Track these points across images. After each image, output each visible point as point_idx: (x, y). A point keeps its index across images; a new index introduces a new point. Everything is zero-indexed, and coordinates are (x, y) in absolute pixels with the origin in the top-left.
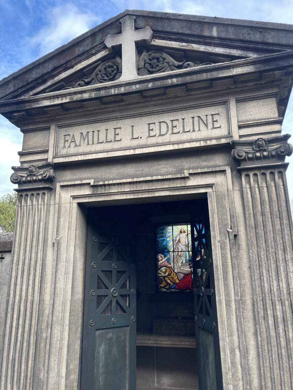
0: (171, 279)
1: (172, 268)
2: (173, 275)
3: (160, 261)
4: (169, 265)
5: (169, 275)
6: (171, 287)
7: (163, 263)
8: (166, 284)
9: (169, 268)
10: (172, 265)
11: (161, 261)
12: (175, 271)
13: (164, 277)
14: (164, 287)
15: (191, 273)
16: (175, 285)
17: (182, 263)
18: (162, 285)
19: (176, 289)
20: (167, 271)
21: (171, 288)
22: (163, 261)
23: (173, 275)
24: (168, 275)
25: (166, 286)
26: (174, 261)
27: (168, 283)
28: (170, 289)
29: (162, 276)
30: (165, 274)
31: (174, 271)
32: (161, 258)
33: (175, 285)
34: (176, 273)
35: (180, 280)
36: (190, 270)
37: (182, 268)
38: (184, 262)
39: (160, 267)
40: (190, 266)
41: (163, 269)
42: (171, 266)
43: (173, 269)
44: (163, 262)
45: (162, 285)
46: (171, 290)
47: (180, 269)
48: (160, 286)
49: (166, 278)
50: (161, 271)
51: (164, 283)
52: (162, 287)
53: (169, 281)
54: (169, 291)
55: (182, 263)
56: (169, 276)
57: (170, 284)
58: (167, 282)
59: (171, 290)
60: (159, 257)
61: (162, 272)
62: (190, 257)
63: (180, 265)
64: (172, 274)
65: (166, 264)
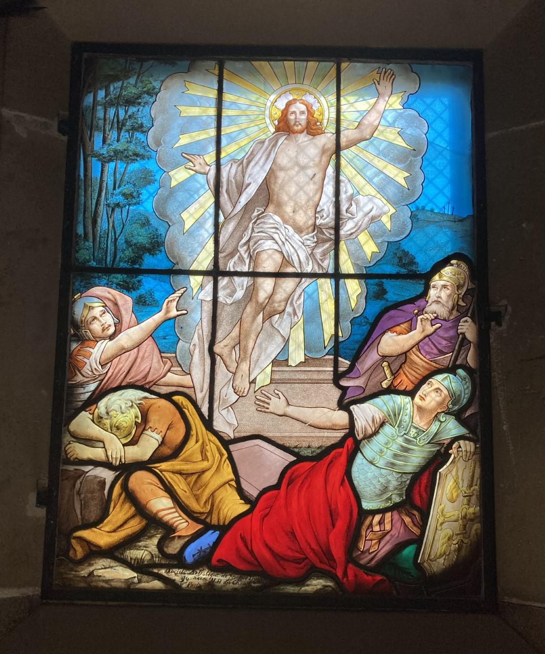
0: (180, 486)
1: (194, 403)
2: (203, 451)
3: (97, 339)
4: (171, 378)
5: (170, 452)
6: (173, 548)
7: (124, 363)
8: (135, 525)
9: (168, 397)
10: (199, 376)
11: (111, 337)
12: (218, 425)
13: (126, 469)
14: (114, 553)
15: (350, 441)
16: (210, 538)
17: (280, 362)
18: (101, 537)
19: (214, 569)
20: (153, 418)
21: (178, 561)
22: (130, 336)
23: (203, 451)
24: (157, 457)
25: (131, 541)
26: (217, 349)
27: (153, 523)
28: (169, 567)
29: (107, 465)
30: (134, 442)
31: (208, 423)
32: (108, 319)
33: (210, 538)
34: (227, 443)
35: (255, 493)
36: (341, 417)
37: (278, 405)
38: (297, 356)
39: (92, 387)
40: (344, 390)
41: (122, 406)
42: (186, 380)
43: (205, 410)
44: (124, 351)
45: (101, 537)
46: (176, 575)
47: (262, 407)
48: (81, 539)
49: (141, 482)
50: (98, 421)
51: (120, 512)
52: (95, 552)
53: (161, 504)
54: (157, 584)
55: (275, 362)
56: (164, 466)
57: (169, 530)
58: (141, 510)
59: (176, 575)
60: (97, 311)
61: (107, 432)
62: (346, 325)
63: (263, 379)
64: (192, 447)
65: (150, 363)
